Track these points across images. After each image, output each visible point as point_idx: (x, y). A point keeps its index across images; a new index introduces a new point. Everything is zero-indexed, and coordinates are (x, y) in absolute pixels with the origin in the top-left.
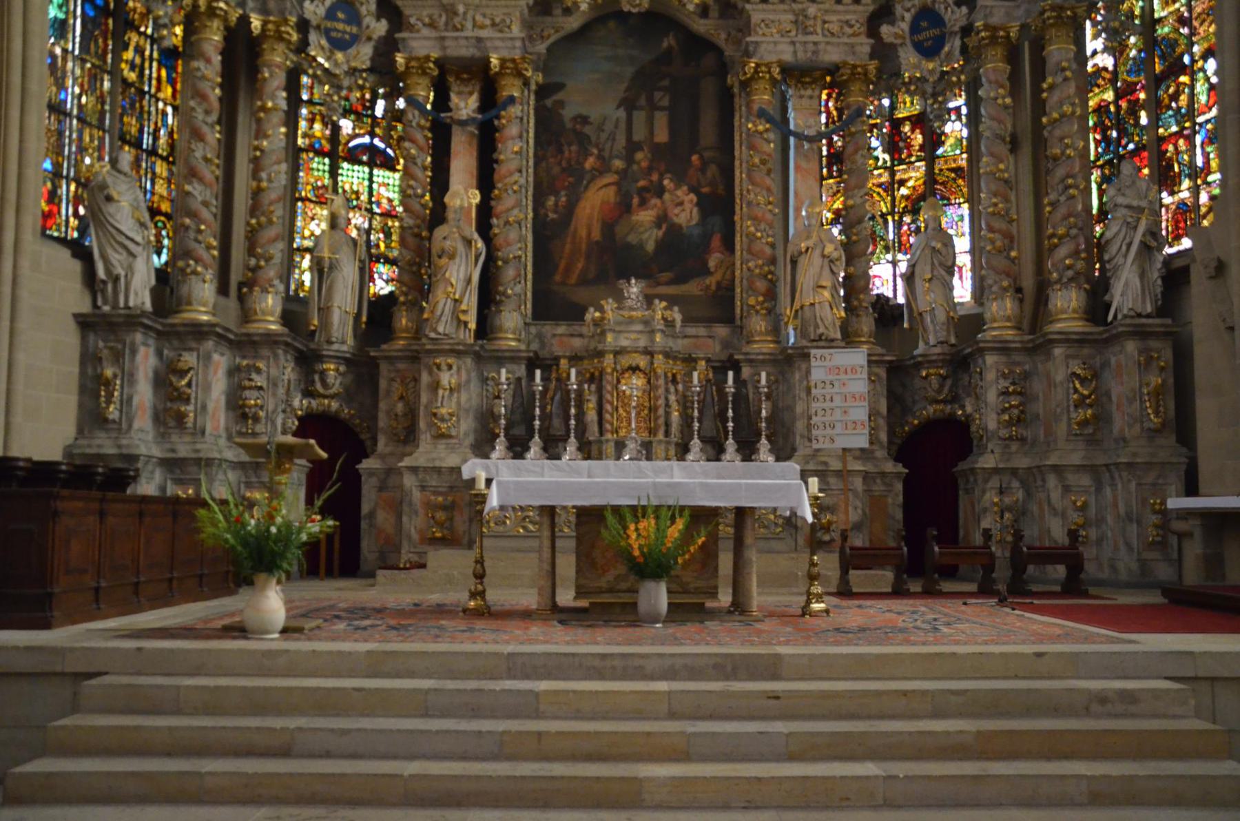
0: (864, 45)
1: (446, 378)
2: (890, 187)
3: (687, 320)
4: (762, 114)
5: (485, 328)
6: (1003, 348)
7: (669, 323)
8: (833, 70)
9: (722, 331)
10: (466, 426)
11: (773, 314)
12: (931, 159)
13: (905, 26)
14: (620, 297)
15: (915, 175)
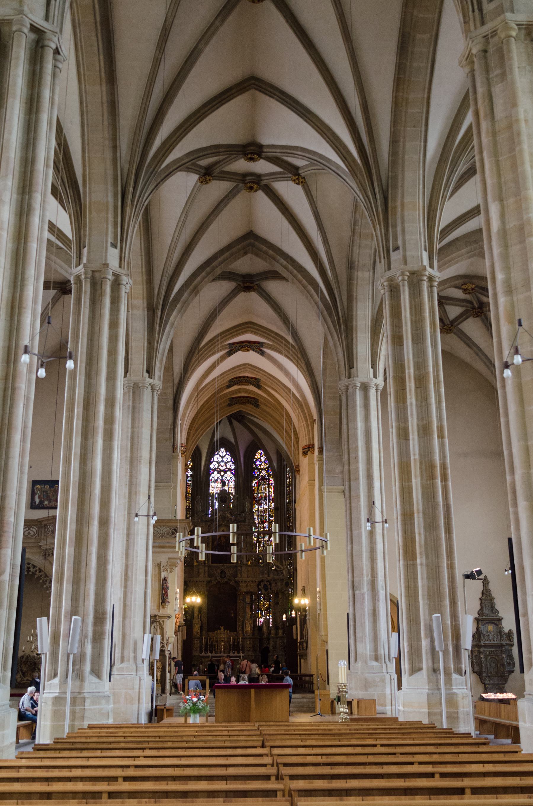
0: (257, 589)
1: (196, 642)
2: (264, 605)
3: (230, 631)
4: (241, 600)
5: (201, 634)
6: (273, 638)
7: (227, 632)
8: (252, 592)
9: (235, 633)
10: (198, 649)
11: (243, 631)
12: (270, 602)
13: (262, 586)
14: (220, 629)
15: (267, 604)
